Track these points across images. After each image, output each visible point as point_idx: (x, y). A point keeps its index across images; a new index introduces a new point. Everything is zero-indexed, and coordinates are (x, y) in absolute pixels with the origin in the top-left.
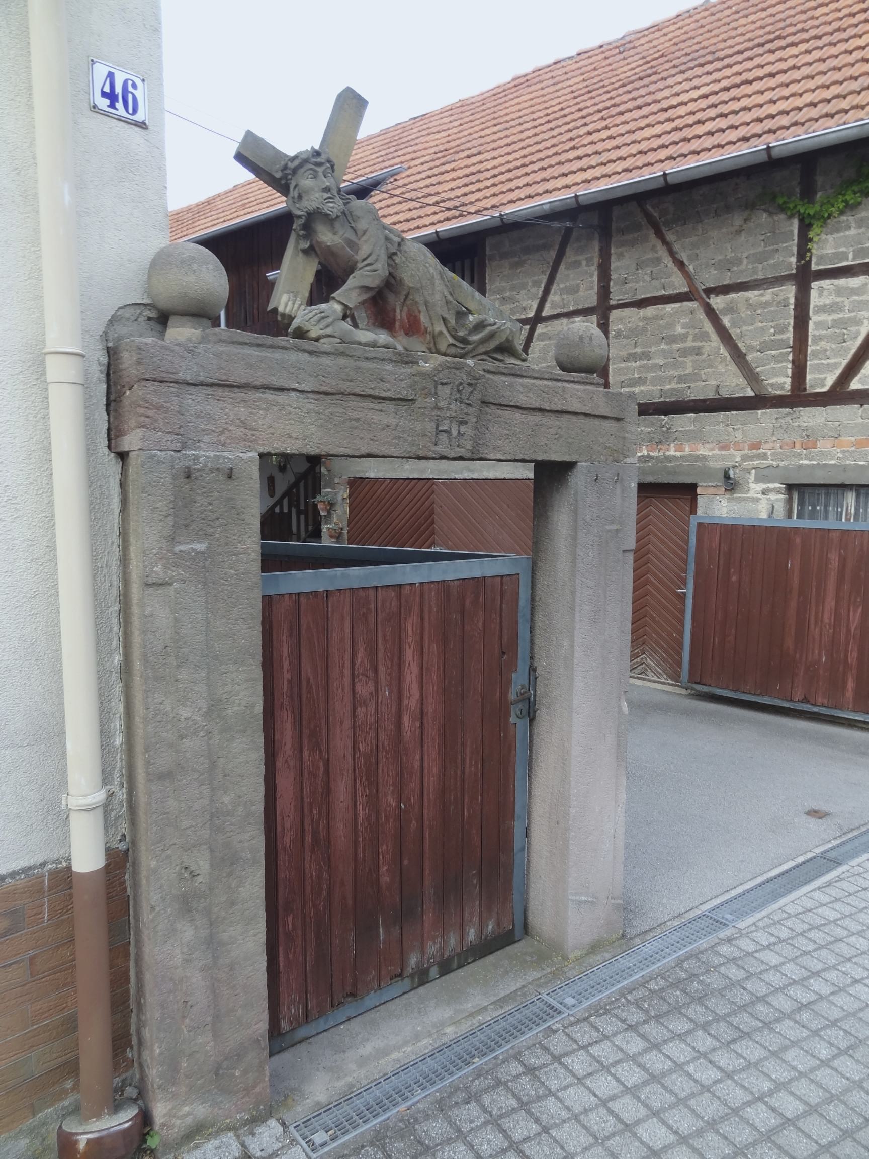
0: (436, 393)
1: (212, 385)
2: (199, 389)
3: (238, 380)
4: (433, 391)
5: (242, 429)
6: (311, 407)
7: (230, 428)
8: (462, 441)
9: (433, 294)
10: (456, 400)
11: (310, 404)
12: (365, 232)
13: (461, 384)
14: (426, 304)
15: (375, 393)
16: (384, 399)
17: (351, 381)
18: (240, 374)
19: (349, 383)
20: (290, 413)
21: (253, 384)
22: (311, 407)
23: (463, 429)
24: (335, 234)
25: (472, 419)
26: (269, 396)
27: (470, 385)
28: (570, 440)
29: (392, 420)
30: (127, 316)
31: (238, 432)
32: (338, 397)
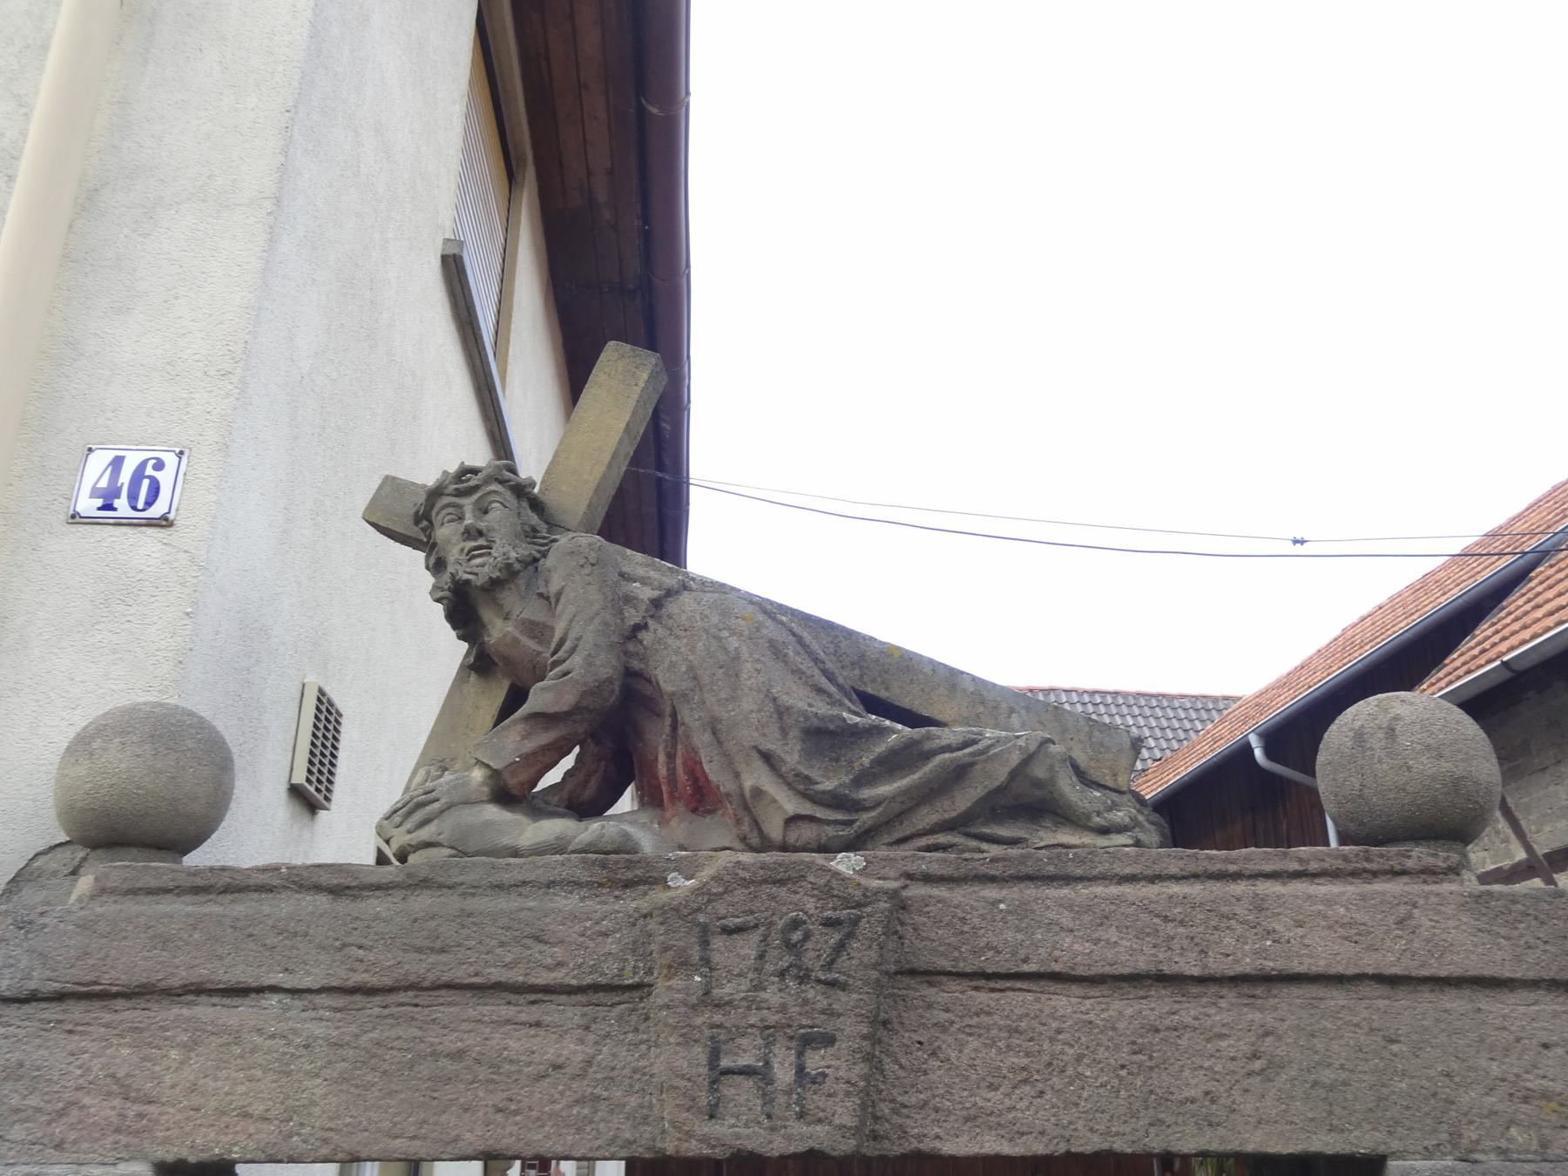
0: (706, 961)
1: (60, 997)
2: (28, 1009)
3: (124, 979)
4: (695, 954)
5: (117, 1102)
6: (319, 1030)
7: (87, 1100)
8: (815, 1101)
9: (733, 698)
10: (782, 974)
11: (318, 1023)
12: (559, 595)
13: (796, 924)
14: (714, 727)
15: (517, 976)
16: (547, 990)
17: (443, 951)
18: (131, 962)
19: (433, 958)
20: (254, 1050)
21: (163, 985)
22: (319, 1030)
23: (815, 1060)
24: (506, 618)
25: (850, 1029)
26: (205, 1011)
27: (830, 923)
28: (1327, 1076)
29: (572, 1050)
30: (53, 866)
31: (102, 1109)
32: (402, 997)
